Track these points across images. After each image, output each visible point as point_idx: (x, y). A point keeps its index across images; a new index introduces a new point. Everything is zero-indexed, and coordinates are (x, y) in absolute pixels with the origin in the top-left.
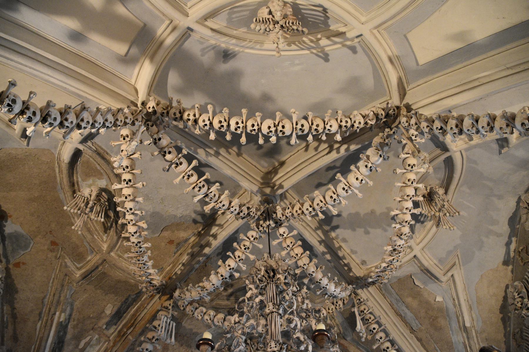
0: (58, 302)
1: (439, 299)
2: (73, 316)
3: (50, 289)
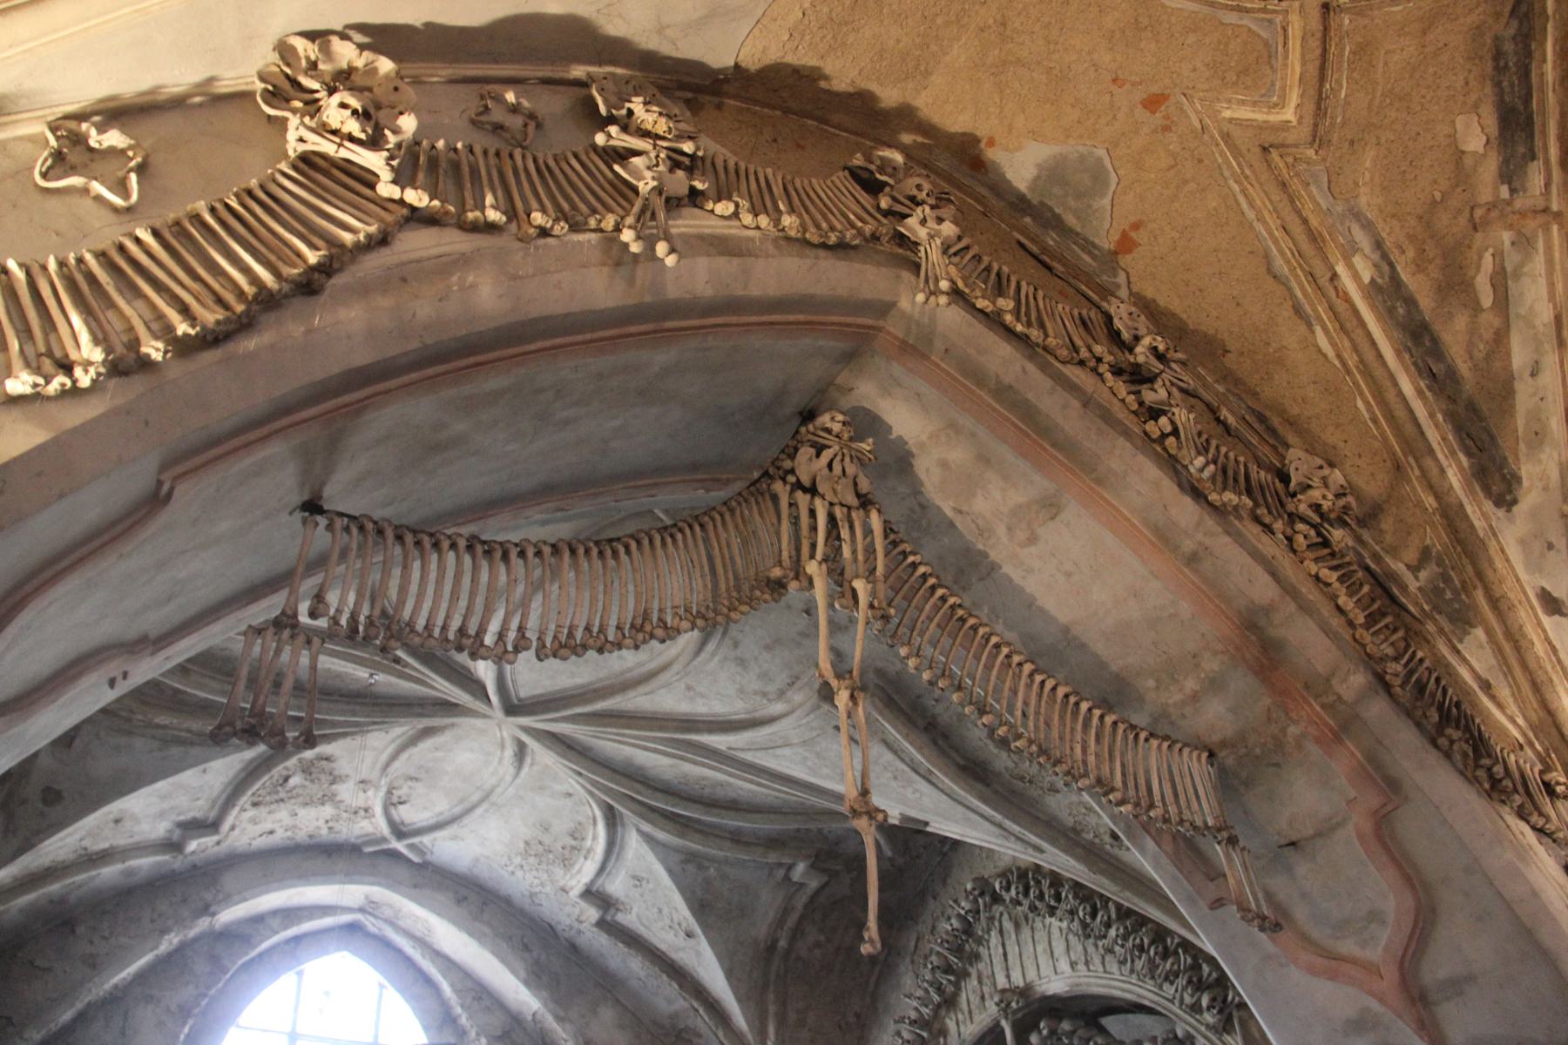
0: (1314, 237)
2: (1388, 243)
3: (1259, 227)
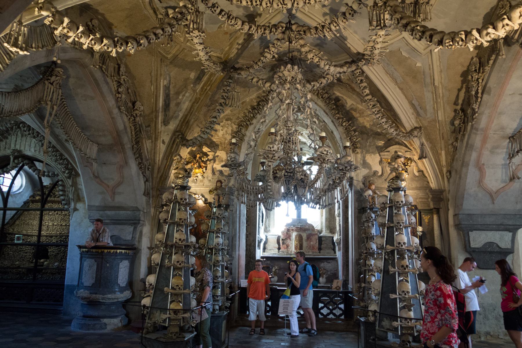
1: (419, 64)
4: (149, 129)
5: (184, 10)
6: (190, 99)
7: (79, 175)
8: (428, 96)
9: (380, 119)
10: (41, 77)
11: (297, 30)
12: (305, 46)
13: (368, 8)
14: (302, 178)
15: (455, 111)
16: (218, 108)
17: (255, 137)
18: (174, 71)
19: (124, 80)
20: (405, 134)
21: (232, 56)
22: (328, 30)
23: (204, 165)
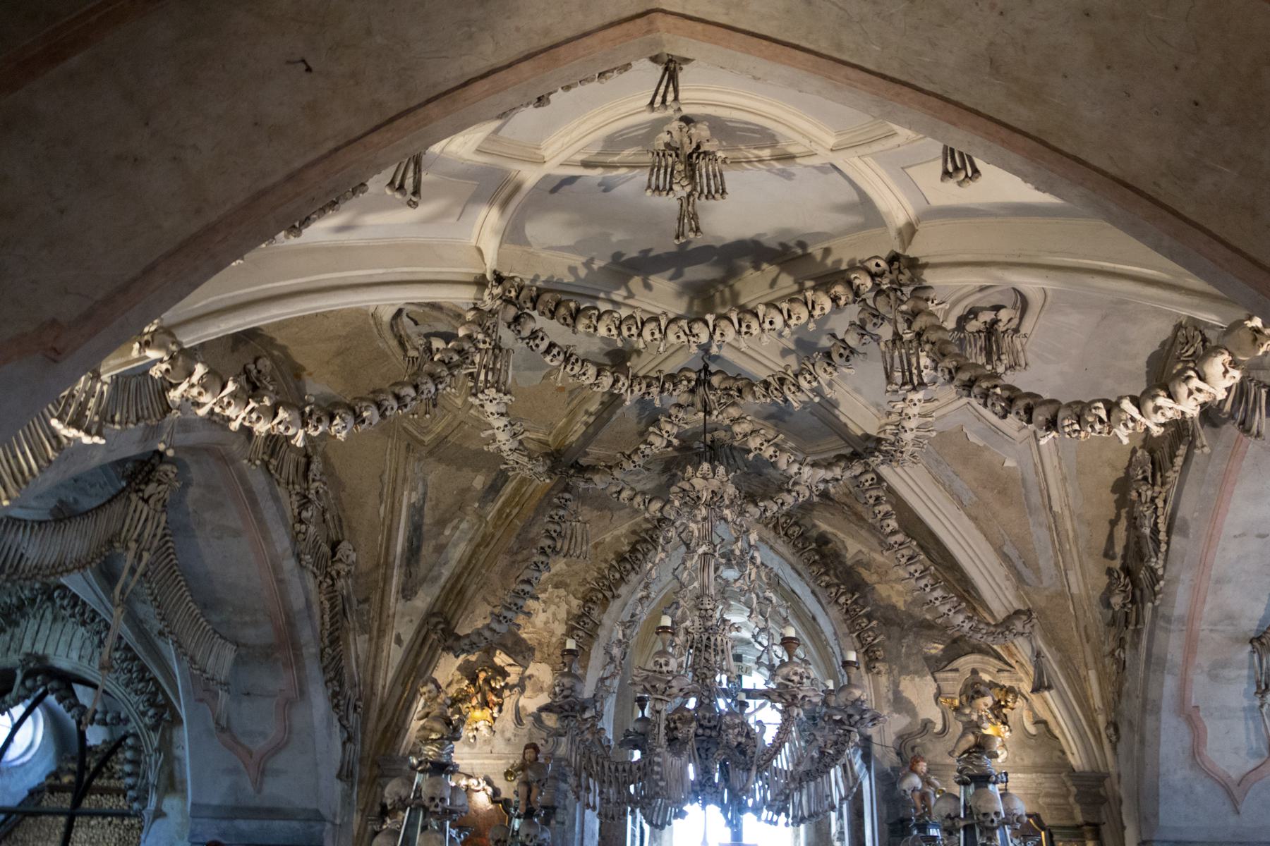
0: (405, 480)
1: (1009, 463)
4: (366, 606)
5: (467, 346)
6: (469, 537)
7: (181, 721)
8: (1040, 536)
9: (928, 589)
10: (124, 484)
11: (723, 386)
12: (743, 423)
13: (882, 344)
14: (740, 744)
15: (1110, 572)
16: (535, 559)
17: (624, 635)
18: (436, 473)
19: (317, 492)
20: (992, 629)
21: (574, 438)
22: (793, 389)
23: (495, 699)
